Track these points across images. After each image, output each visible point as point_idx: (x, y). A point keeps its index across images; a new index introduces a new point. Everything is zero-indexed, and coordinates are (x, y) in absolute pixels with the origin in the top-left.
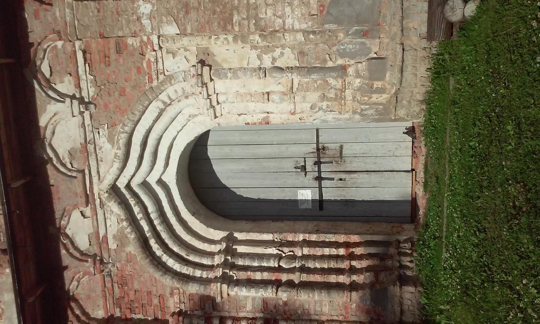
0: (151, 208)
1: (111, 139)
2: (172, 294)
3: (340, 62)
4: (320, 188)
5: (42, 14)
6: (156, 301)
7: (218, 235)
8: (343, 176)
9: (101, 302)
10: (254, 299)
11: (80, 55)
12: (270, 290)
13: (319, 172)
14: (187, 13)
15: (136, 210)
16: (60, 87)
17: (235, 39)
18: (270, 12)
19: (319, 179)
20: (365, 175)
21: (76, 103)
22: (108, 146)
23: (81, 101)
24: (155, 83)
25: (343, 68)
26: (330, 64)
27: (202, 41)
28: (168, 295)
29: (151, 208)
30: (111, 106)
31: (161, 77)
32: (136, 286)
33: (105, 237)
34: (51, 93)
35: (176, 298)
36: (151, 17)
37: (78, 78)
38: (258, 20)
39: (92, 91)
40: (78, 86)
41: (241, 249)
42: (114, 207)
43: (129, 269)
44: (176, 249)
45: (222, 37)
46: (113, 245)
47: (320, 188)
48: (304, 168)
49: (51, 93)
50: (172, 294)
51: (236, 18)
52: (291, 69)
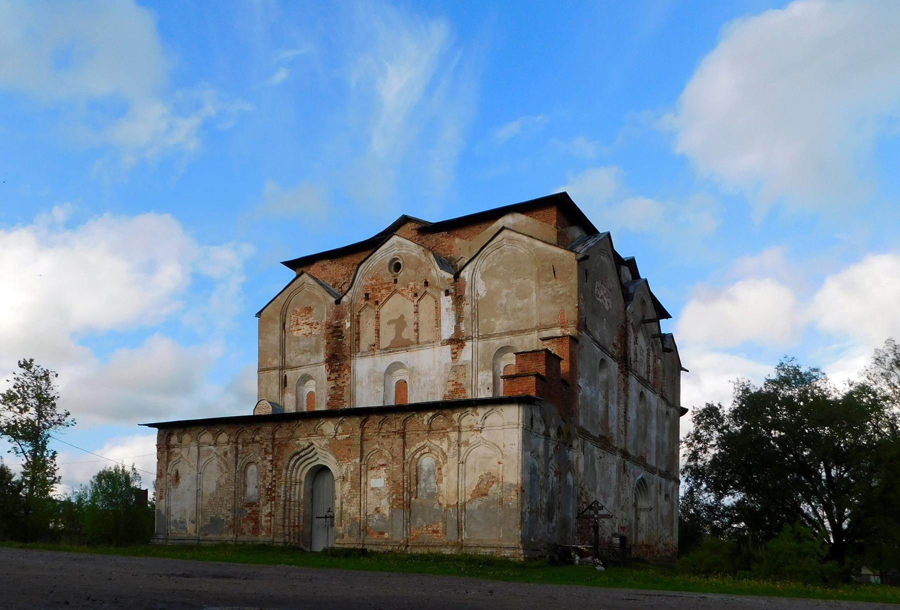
0: (309, 455)
1: (326, 444)
2: (283, 463)
3: (343, 525)
4: (323, 517)
5: (358, 425)
6: (281, 457)
7: (303, 479)
8: (327, 526)
9: (280, 437)
10: (281, 492)
11: (348, 436)
12: (284, 498)
13: (328, 517)
14: (356, 475)
15: (307, 451)
16: (340, 427)
17: (350, 490)
18: (355, 502)
19: (326, 517)
20: (327, 535)
21: (334, 434)
22: (324, 443)
23: (335, 435)
24: (339, 462)
25: (341, 525)
26: (343, 521)
27: (349, 480)
28: (283, 461)
29: (309, 455)
30: (335, 445)
31: (341, 464)
32: (285, 450)
33: (299, 440)
34: (337, 425)
35: (281, 465)
36: (355, 462)
37: (342, 434)
38: (354, 497)
39: (339, 439)
40: (340, 435)
41: (298, 487)
42: (307, 445)
43: (290, 448)
44: (297, 464)
45: (350, 486)
46: (297, 442)
47: (323, 517)
48: (329, 511)
49: (337, 425)
50: (283, 463)
51: (354, 491)
52: (342, 508)
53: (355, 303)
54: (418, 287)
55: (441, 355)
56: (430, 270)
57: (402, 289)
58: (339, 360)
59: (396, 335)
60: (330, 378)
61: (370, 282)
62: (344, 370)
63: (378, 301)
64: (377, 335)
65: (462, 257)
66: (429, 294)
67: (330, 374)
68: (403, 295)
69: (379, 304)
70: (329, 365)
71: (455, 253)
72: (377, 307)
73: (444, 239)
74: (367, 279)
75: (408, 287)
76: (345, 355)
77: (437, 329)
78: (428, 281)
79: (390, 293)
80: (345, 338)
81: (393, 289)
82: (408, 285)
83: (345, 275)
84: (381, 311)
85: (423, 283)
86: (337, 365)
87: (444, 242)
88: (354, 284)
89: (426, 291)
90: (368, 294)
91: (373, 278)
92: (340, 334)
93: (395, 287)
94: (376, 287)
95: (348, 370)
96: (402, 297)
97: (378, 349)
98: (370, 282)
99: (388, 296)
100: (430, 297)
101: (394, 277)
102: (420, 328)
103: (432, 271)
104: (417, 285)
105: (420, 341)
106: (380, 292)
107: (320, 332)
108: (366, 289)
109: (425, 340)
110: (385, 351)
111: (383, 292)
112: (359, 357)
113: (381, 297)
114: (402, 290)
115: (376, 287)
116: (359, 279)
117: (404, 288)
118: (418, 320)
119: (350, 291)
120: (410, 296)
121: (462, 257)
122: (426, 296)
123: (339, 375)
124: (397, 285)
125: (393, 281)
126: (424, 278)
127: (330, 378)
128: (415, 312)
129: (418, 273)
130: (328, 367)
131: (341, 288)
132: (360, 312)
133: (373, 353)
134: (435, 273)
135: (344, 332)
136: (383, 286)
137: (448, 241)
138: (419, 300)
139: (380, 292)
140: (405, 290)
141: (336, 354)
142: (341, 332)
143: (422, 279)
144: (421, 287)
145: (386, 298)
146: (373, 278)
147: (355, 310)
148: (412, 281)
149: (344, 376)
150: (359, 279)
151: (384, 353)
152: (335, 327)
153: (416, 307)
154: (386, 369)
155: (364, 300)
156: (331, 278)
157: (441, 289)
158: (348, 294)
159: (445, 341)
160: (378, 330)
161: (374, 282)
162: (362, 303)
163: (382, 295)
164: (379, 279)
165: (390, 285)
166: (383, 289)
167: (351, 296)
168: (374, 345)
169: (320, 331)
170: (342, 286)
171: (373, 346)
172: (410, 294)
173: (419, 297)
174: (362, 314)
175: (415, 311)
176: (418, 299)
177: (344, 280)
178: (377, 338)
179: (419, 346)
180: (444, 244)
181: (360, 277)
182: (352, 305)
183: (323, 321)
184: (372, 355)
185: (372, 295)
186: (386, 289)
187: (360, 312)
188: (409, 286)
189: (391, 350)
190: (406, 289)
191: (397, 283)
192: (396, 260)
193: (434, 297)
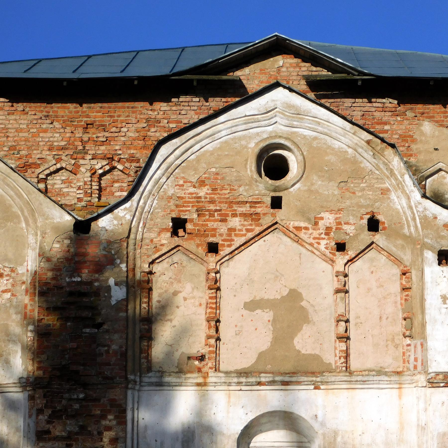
53: (139, 237)
54: (350, 229)
55: (426, 410)
56: (385, 192)
57: (297, 224)
58: (85, 386)
59: (276, 341)
60: (48, 432)
61: (192, 190)
62: (103, 417)
63: (217, 244)
64: (213, 332)
65: (440, 170)
66: (381, 249)
67: (48, 422)
68: (298, 241)
69: (222, 253)
70: (45, 396)
71: (421, 157)
72: (212, 259)
73: (387, 116)
74: (181, 182)
75: (316, 224)
76: (108, 373)
77: (408, 341)
78: (380, 217)
79: (258, 230)
80: (105, 327)
81: (267, 221)
82: (315, 218)
83: (63, 148)
84: (225, 270)
85: (365, 222)
86: (78, 400)
87: (385, 123)
88: (141, 189)
89: (373, 243)
90: (185, 221)
91: (202, 183)
92: (86, 313)
93: (273, 215)
94: (212, 207)
95: (116, 417)
96: (295, 244)
97: (217, 369)
98: (192, 190)
99: (250, 235)
100: (383, 259)
101: (275, 191)
102: (352, 334)
103: (393, 196)
104: (347, 223)
105: (354, 364)
106: (224, 220)
107: (10, 300)
108: (177, 206)
109: (370, 364)
110: (243, 380)
111: (235, 222)
112: (151, 384)
113: (230, 235)
114: (298, 229)
115: (212, 207)
116: (156, 176)
117: (303, 224)
118: (347, 309)
119: (127, 205)
120: (322, 247)
121: (440, 170)
122: (372, 254)
123: (83, 428)
124: (280, 215)
125: (268, 201)
126: (369, 210)
127: (48, 432)
128: (338, 291)
129: (348, 194)
130: (40, 402)
131: (45, 180)
132: (152, 262)
133: (200, 380)
134: (404, 202)
135: (103, 312)
136: (235, 207)
137: (401, 123)
138: (351, 261)
139: (224, 220)
140: (306, 228)
141: (74, 368)
142: (93, 308)
143: (363, 211)
144: (359, 229)
145: (243, 240)
146: (202, 183)
147: (138, 256)
148: (331, 211)
149: (100, 434)
150: (156, 176)
151: (239, 383)
152: (71, 294)
153: (341, 278)
154: (242, 428)
155: (169, 234)
156: (12, 148)
157: (425, 246)
158: (120, 211)
159: (441, 377)
160: (218, 321)
161: (203, 192)
162: (164, 242)
163: (231, 230)
164: (223, 188)
165: (259, 210)
166: (234, 215)
167: (128, 217)
168: (202, 358)
169: (8, 295)
170: (48, 175)
171: (197, 358)
172: (323, 242)
173: (351, 254)
174: (156, 268)
175: (341, 287)
176: (347, 258)
177: (59, 160)
178: (212, 341)
179: (354, 378)
180: (387, 127)
181: (159, 172)
182: (131, 242)
183: (21, 270)
184: (198, 385)
185: (195, 225)
186: (244, 215)
187: (152, 262)
188: (321, 223)
189: (263, 380)
190: (310, 226)
191: (280, 207)
192: (277, 148)
193: (397, 261)
